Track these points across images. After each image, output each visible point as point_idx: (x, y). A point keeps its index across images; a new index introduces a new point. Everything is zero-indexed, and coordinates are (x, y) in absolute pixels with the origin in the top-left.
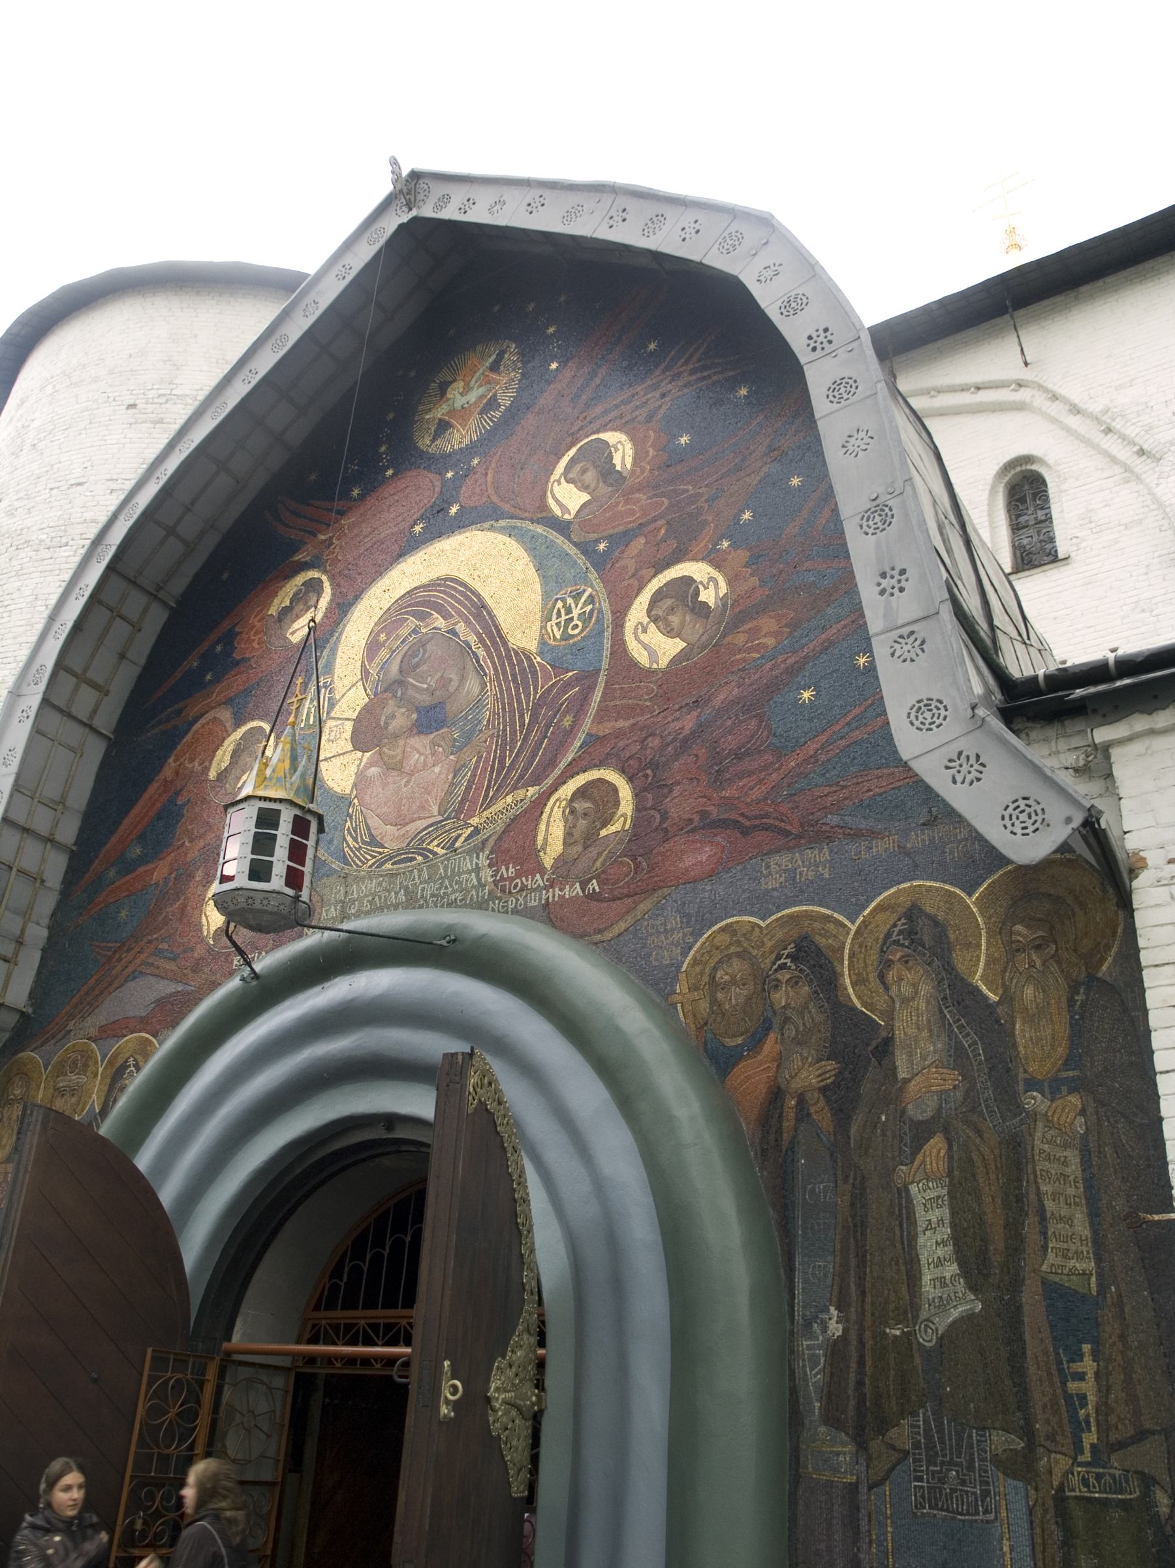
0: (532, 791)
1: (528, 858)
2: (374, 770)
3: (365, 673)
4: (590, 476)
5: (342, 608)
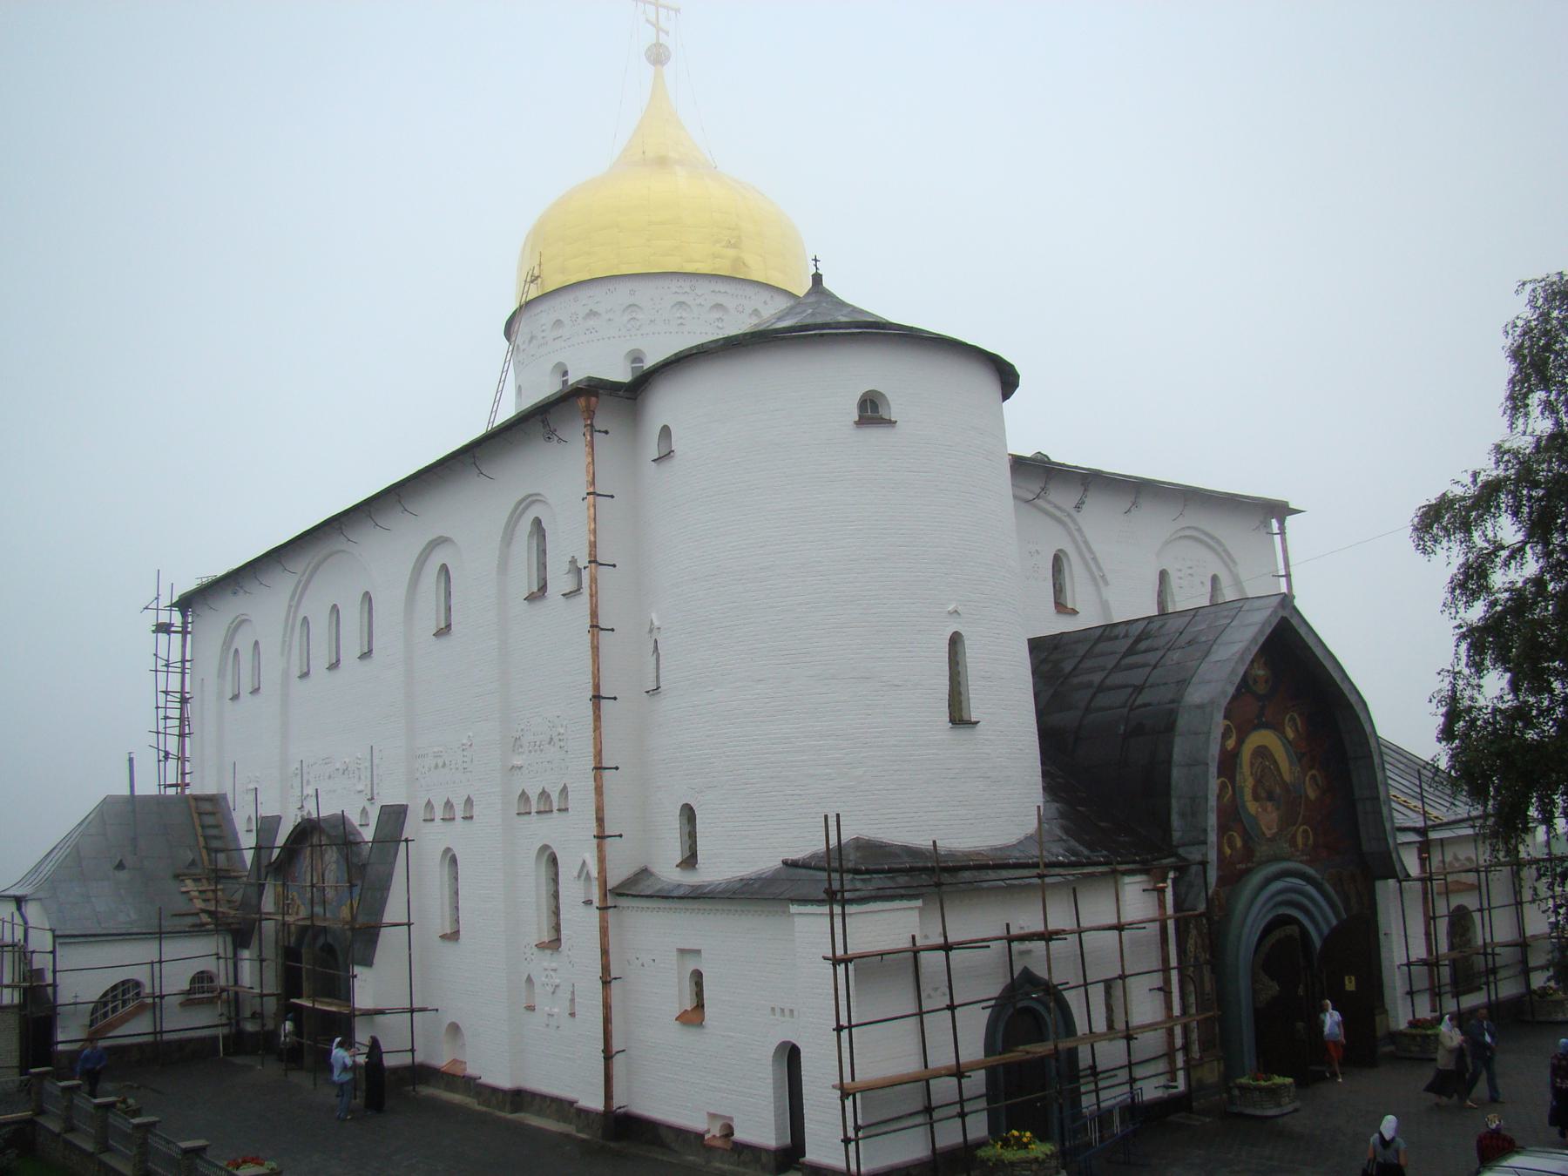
0: (1295, 828)
3: (1251, 773)
5: (1240, 742)
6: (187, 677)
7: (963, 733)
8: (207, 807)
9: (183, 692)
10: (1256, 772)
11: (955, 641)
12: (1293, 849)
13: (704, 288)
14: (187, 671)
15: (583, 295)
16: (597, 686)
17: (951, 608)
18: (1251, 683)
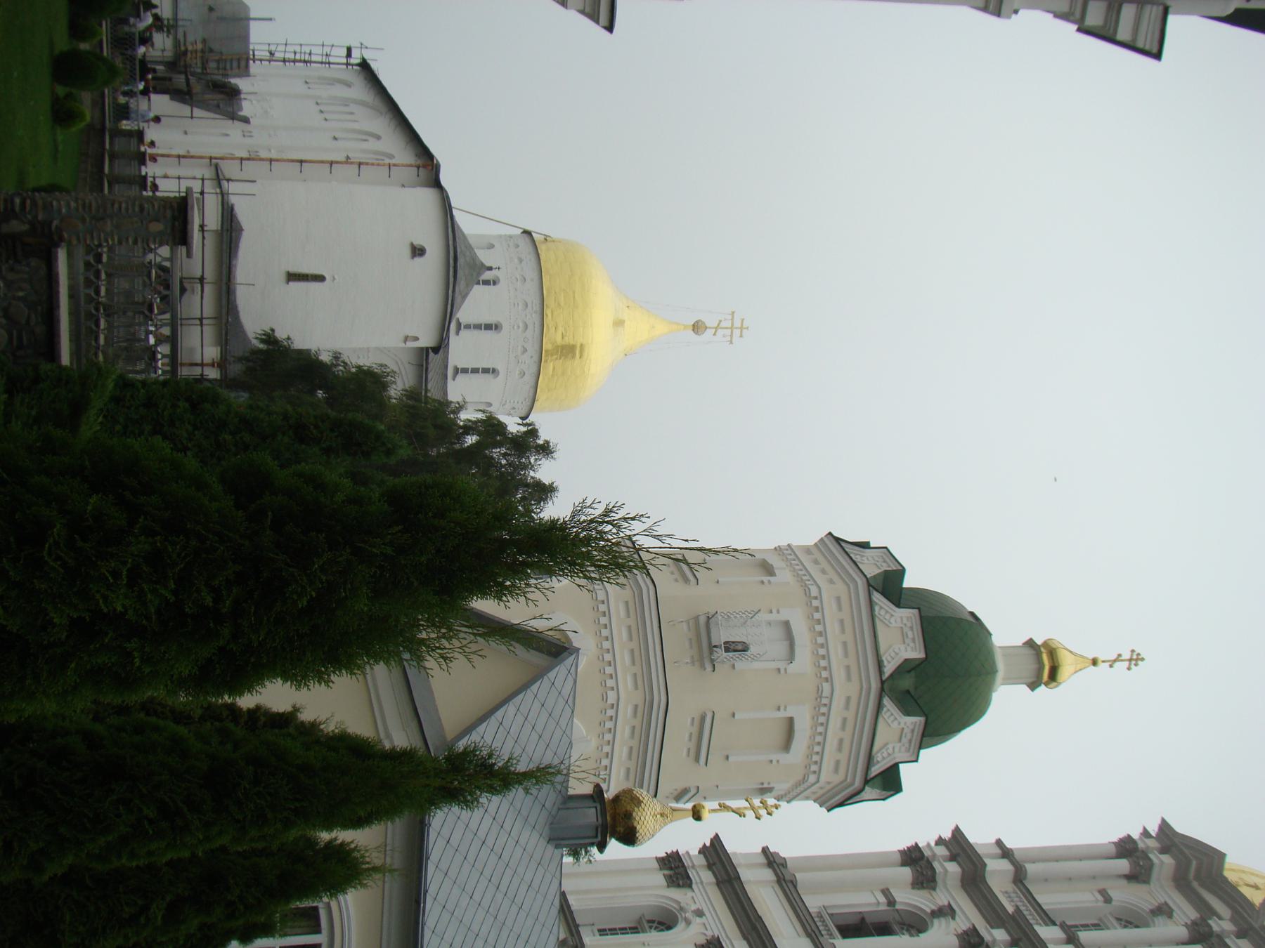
6: (319, 65)
7: (283, 277)
8: (243, 64)
9: (311, 62)
11: (320, 278)
13: (536, 318)
14: (324, 65)
15: (533, 257)
16: (306, 161)
17: (336, 277)
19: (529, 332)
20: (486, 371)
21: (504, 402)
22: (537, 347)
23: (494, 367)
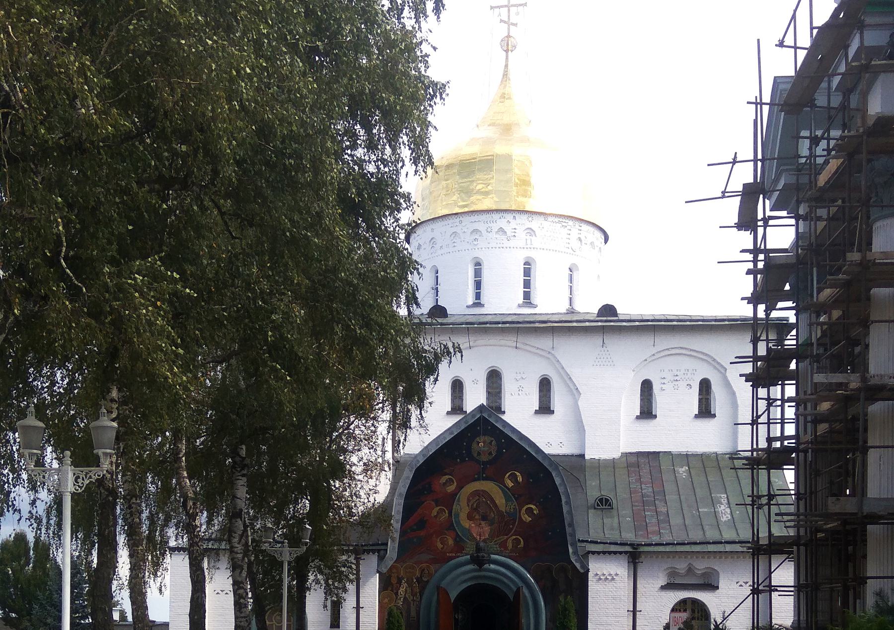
1: (506, 548)
2: (473, 525)
4: (513, 480)
5: (460, 487)
10: (472, 505)
12: (503, 549)
13: (466, 219)
18: (475, 455)
19: (482, 227)
20: (527, 272)
21: (573, 252)
22: (496, 216)
23: (523, 264)
